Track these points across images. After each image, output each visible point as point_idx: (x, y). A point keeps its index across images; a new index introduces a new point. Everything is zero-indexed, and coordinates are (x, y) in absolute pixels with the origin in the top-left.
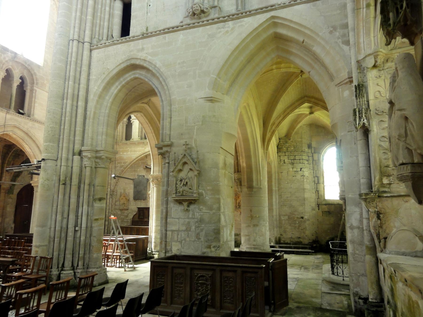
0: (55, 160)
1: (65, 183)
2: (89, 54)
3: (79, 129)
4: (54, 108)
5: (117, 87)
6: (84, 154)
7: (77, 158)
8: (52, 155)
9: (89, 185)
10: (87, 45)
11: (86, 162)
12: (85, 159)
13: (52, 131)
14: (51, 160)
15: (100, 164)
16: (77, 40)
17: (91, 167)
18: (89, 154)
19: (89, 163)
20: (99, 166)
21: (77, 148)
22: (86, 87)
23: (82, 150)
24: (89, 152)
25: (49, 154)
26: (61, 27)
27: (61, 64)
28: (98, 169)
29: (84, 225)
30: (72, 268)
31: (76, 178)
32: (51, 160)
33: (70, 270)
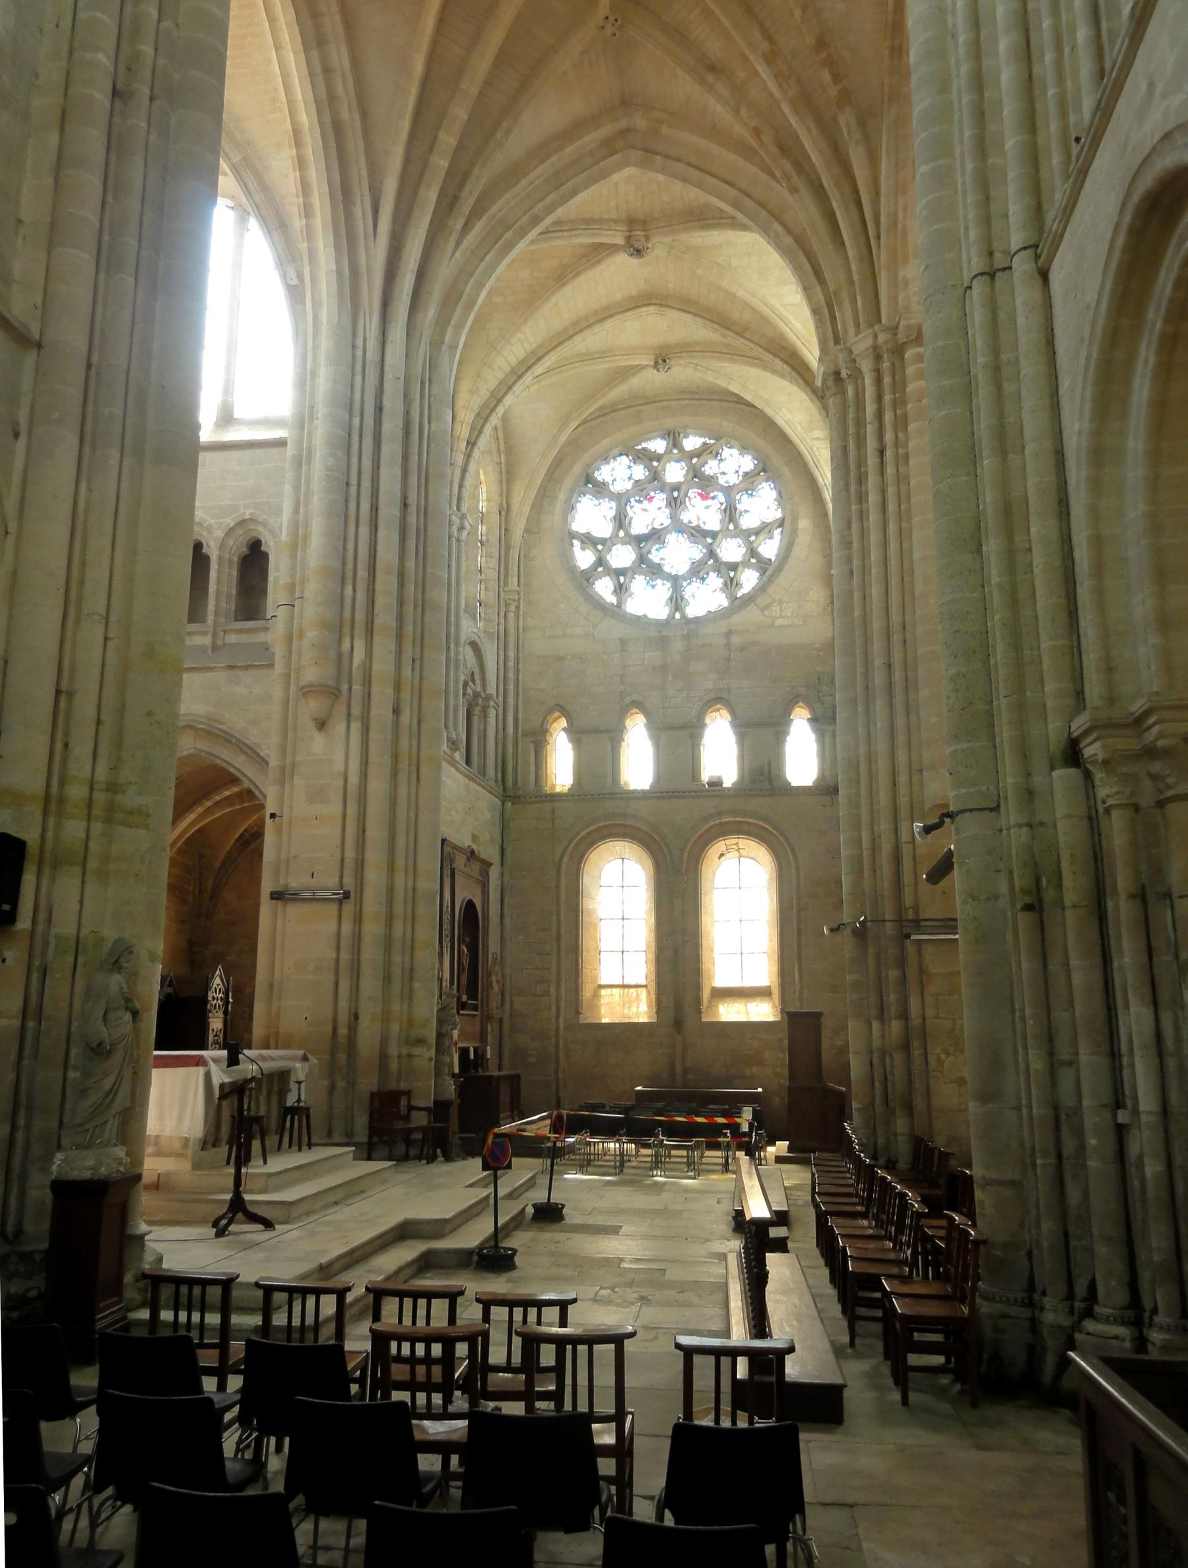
0: (991, 810)
1: (1040, 900)
2: (1037, 295)
3: (1052, 643)
4: (950, 598)
5: (1146, 361)
6: (1091, 750)
7: (1063, 777)
8: (972, 790)
9: (1141, 896)
10: (1022, 265)
11: (1106, 789)
12: (1099, 775)
13: (957, 691)
14: (971, 810)
15: (1171, 781)
16: (982, 274)
17: (1137, 808)
18: (1098, 744)
19: (1115, 789)
20: (1170, 793)
21: (1054, 731)
22: (1048, 445)
23: (1075, 735)
24: (1094, 735)
25: (963, 791)
26: (927, 267)
27: (943, 413)
28: (1171, 808)
29: (1147, 1102)
30: (1130, 1314)
31: (1074, 873)
32: (971, 810)
33: (1116, 1321)
